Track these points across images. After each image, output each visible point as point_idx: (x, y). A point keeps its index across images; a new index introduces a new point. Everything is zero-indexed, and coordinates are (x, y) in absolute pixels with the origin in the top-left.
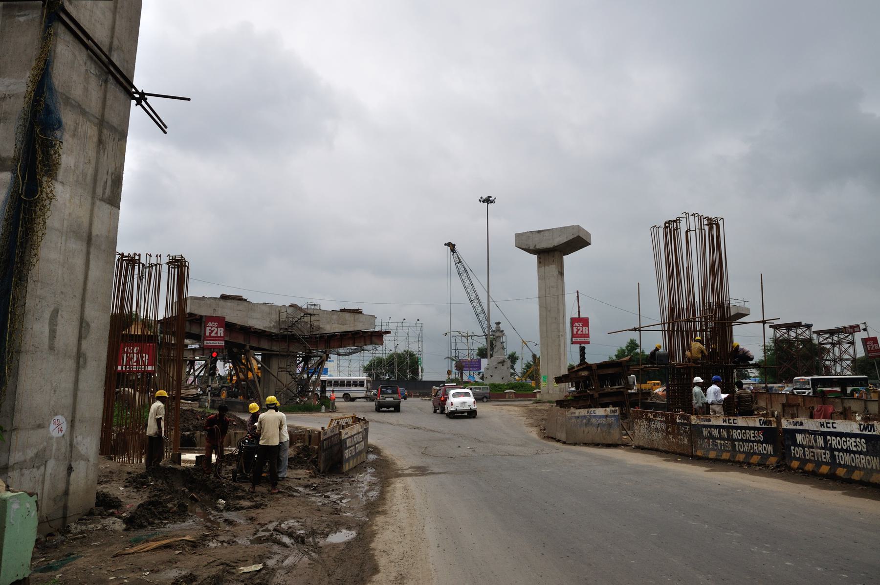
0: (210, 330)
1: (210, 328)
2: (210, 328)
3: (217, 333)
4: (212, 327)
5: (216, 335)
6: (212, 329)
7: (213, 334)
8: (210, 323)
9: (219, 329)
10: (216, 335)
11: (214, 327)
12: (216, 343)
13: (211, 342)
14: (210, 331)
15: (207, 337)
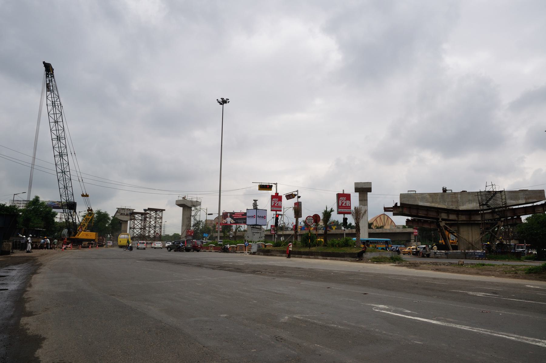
0: (341, 202)
1: (341, 201)
2: (341, 201)
3: (346, 204)
5: (345, 205)
6: (343, 202)
7: (343, 205)
8: (341, 198)
10: (345, 205)
11: (344, 200)
13: (343, 210)
14: (342, 203)
15: (340, 206)
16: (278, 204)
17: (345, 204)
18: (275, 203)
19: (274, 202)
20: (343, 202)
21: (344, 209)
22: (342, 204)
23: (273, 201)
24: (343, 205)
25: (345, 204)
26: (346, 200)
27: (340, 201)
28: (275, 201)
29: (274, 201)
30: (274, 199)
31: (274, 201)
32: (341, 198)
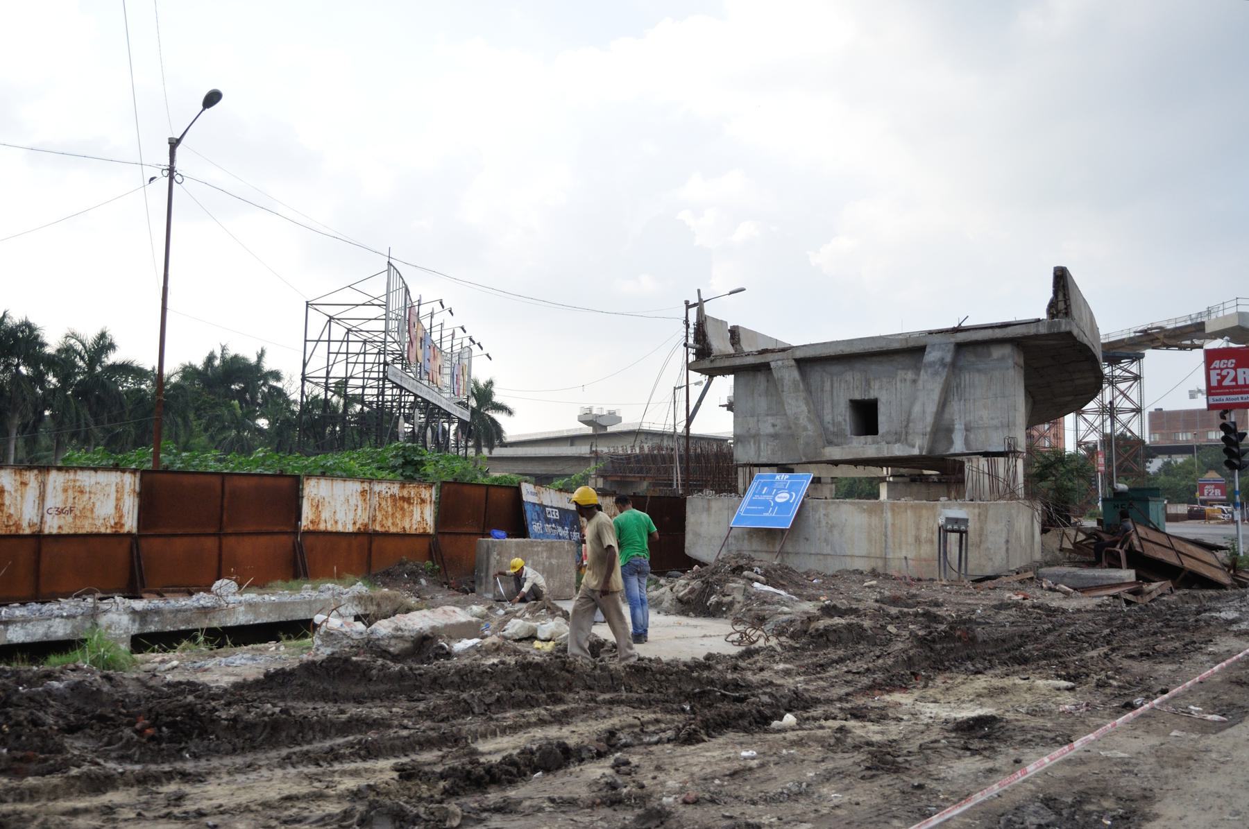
0: (1218, 374)
3: (1235, 379)
4: (1222, 369)
5: (1234, 383)
7: (1226, 382)
9: (1238, 370)
10: (1234, 383)
11: (1227, 368)
12: (1235, 399)
13: (1224, 397)
14: (1219, 377)
16: (1235, 379)
17: (1231, 381)
18: (1224, 378)
19: (1218, 374)
20: (1224, 373)
21: (1228, 397)
22: (1220, 382)
23: (1215, 369)
24: (1226, 382)
25: (1231, 381)
26: (1235, 369)
27: (1213, 373)
28: (1222, 369)
29: (1219, 371)
30: (1218, 362)
31: (1219, 371)
32: (1216, 364)
